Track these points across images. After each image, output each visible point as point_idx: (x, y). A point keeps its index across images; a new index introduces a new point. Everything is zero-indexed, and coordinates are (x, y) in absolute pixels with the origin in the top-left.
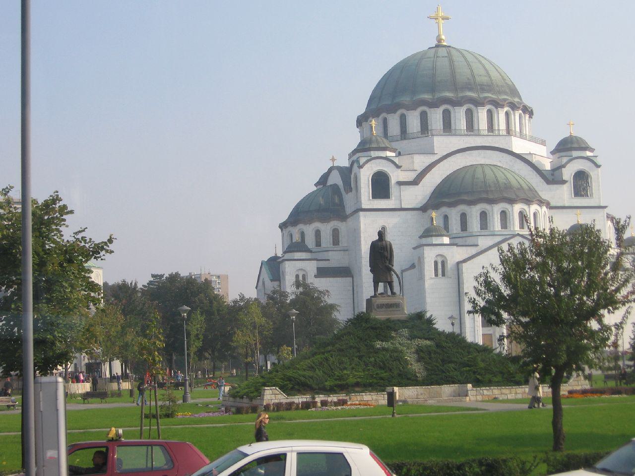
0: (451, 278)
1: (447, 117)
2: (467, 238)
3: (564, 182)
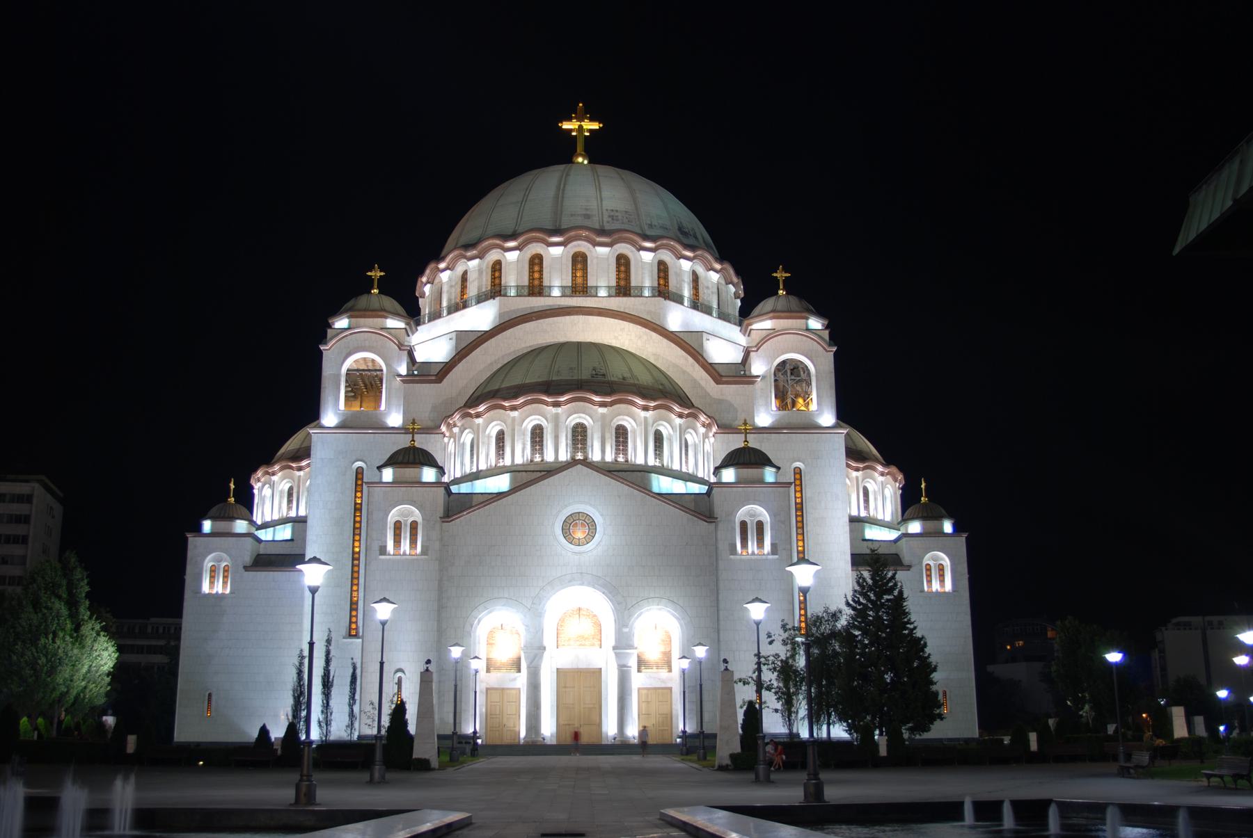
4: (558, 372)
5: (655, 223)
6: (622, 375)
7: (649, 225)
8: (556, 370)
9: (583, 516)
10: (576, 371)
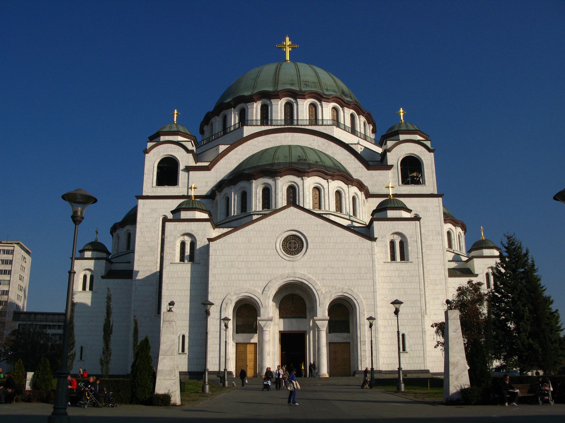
0: (199, 263)
1: (265, 111)
2: (242, 220)
3: (390, 167)
4: (278, 158)
5: (329, 88)
6: (315, 160)
7: (326, 89)
8: (276, 157)
9: (294, 238)
10: (288, 158)
